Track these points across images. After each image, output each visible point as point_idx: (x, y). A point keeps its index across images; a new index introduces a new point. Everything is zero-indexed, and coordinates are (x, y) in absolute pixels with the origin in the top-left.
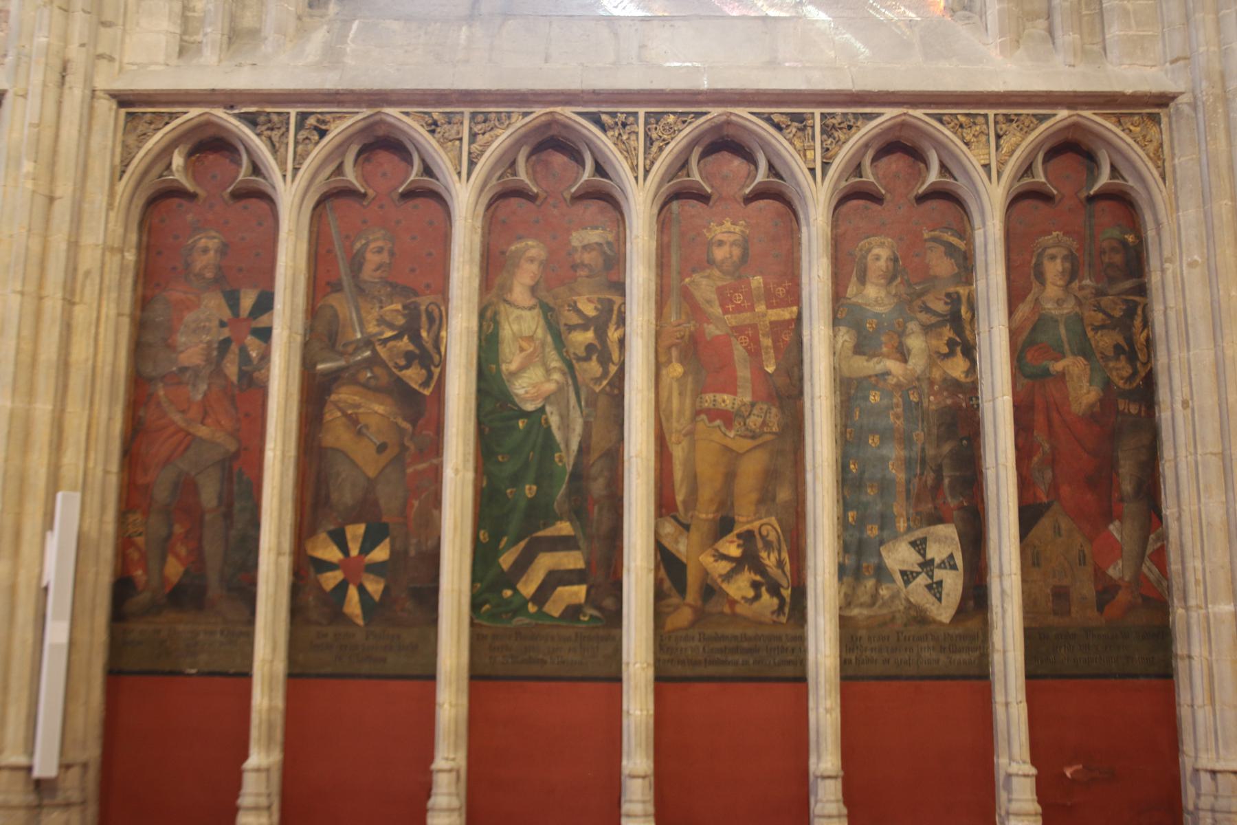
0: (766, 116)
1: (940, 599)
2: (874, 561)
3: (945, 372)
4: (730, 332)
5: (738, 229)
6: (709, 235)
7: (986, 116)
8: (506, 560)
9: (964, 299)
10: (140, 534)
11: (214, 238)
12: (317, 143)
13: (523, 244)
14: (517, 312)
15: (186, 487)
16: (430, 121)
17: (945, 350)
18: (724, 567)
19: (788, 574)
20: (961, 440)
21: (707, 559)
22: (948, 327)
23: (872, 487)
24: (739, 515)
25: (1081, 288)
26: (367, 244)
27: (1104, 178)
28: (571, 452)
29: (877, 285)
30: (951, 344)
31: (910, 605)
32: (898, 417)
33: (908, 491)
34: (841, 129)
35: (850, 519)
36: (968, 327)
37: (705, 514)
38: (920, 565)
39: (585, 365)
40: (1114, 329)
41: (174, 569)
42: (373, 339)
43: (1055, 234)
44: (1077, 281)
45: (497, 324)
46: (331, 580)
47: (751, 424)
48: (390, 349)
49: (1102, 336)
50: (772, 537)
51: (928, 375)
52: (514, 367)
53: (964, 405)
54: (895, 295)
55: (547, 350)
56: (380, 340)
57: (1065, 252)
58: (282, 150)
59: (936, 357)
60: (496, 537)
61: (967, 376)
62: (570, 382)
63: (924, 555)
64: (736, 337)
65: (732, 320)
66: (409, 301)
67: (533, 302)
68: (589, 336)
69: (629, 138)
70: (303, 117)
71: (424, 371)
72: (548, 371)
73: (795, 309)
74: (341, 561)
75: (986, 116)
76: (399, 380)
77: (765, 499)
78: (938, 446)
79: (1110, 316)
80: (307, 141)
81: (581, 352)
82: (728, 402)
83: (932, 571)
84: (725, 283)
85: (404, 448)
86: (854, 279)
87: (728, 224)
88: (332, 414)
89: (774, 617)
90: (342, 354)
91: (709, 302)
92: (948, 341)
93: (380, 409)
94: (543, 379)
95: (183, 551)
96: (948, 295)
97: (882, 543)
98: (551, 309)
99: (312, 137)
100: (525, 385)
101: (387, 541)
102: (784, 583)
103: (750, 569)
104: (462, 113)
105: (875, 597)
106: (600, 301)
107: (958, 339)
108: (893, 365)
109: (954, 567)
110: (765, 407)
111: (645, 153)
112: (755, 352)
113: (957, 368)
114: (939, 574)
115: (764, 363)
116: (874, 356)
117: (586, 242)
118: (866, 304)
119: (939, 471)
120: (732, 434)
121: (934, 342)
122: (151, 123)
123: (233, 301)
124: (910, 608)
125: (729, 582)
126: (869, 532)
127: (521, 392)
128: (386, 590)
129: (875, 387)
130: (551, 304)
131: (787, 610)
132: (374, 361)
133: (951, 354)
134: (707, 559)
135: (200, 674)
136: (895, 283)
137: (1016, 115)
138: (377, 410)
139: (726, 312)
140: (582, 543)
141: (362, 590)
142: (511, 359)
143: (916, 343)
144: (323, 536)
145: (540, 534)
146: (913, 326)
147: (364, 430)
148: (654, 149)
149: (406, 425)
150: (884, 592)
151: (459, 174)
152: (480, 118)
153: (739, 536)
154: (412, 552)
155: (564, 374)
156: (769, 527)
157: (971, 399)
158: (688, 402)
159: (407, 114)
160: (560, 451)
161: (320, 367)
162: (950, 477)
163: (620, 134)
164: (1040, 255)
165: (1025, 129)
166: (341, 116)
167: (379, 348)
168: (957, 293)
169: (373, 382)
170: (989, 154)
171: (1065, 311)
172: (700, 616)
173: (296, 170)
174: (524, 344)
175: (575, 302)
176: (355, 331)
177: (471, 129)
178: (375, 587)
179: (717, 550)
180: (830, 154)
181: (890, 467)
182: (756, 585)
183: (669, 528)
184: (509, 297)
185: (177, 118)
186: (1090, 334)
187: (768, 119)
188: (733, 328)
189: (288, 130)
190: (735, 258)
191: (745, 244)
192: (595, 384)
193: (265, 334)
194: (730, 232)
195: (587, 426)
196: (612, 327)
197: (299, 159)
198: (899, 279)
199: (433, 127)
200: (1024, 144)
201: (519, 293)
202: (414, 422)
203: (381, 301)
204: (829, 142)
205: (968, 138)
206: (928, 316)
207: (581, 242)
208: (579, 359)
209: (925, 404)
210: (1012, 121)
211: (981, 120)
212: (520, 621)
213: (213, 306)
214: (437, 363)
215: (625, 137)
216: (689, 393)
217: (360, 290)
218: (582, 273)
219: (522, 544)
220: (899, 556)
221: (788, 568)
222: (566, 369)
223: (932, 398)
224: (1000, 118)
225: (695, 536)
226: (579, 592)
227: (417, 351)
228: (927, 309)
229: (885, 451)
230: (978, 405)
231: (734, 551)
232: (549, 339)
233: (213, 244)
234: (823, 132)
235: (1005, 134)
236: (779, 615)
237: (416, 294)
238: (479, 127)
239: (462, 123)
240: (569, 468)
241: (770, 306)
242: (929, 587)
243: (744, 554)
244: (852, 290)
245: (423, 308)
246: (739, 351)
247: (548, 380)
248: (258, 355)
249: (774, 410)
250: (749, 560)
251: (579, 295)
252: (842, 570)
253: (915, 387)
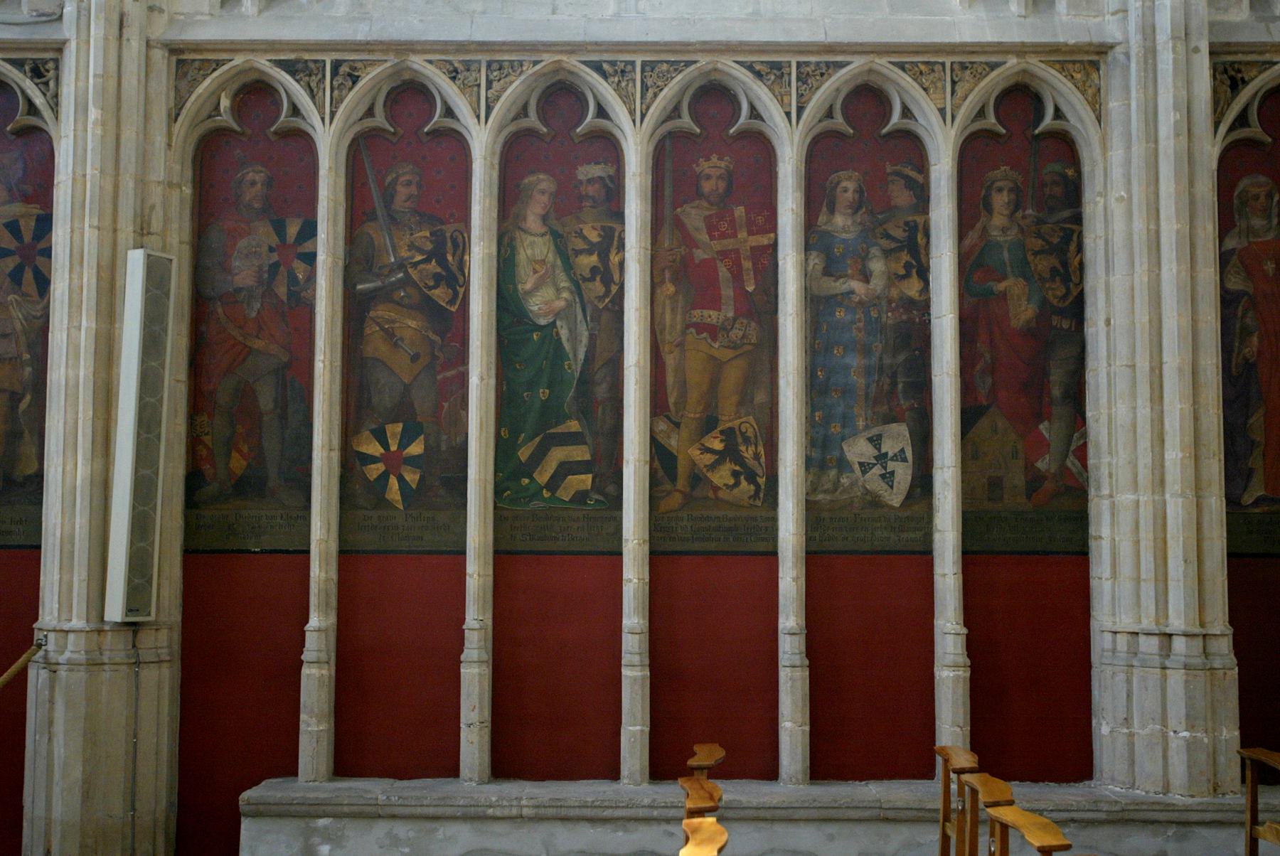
0: (749, 64)
1: (892, 487)
2: (836, 454)
3: (902, 292)
4: (716, 256)
5: (723, 164)
6: (698, 170)
7: (943, 64)
8: (524, 454)
9: (921, 227)
10: (207, 434)
11: (261, 172)
12: (350, 89)
13: (535, 178)
14: (530, 239)
15: (246, 394)
16: (451, 69)
17: (902, 272)
18: (709, 459)
19: (764, 465)
20: (914, 351)
21: (695, 453)
22: (906, 252)
23: (836, 391)
24: (722, 415)
25: (1024, 217)
26: (397, 178)
27: (1048, 121)
28: (579, 360)
29: (844, 215)
30: (908, 266)
31: (868, 492)
32: (859, 330)
33: (867, 395)
34: (814, 76)
35: (817, 419)
36: (923, 251)
37: (693, 413)
38: (876, 458)
39: (590, 285)
40: (1051, 254)
41: (238, 464)
42: (406, 263)
43: (1003, 168)
44: (1021, 211)
45: (513, 249)
46: (374, 470)
47: (734, 337)
48: (420, 272)
49: (1040, 260)
50: (750, 433)
51: (887, 294)
52: (528, 286)
53: (917, 320)
54: (860, 224)
55: (558, 272)
56: (411, 263)
57: (1011, 185)
58: (321, 94)
59: (894, 278)
60: (515, 433)
61: (920, 296)
62: (577, 300)
63: (879, 450)
64: (722, 261)
65: (717, 245)
66: (435, 229)
67: (543, 230)
68: (594, 259)
69: (627, 85)
70: (336, 65)
72: (558, 290)
73: (772, 235)
74: (382, 454)
75: (943, 64)
76: (429, 298)
77: (745, 400)
78: (894, 356)
79: (1047, 241)
80: (342, 86)
81: (587, 274)
82: (713, 317)
83: (886, 463)
84: (711, 213)
85: (434, 357)
86: (824, 209)
87: (714, 158)
88: (371, 329)
89: (751, 502)
90: (378, 276)
91: (697, 229)
92: (905, 264)
94: (554, 298)
95: (245, 449)
96: (906, 224)
97: (843, 439)
98: (560, 236)
99: (346, 83)
100: (538, 303)
101: (422, 437)
102: (759, 472)
103: (730, 461)
104: (479, 62)
105: (837, 484)
106: (603, 228)
107: (914, 262)
108: (856, 285)
109: (905, 460)
110: (745, 321)
111: (642, 98)
112: (737, 276)
113: (912, 288)
114: (891, 466)
115: (745, 284)
116: (841, 277)
117: (590, 176)
118: (834, 231)
119: (894, 376)
120: (716, 345)
121: (893, 265)
122: (200, 70)
123: (280, 229)
124: (866, 494)
125: (713, 471)
126: (833, 430)
127: (536, 308)
128: (422, 479)
129: (840, 305)
130: (560, 231)
131: (761, 495)
132: (407, 282)
133: (907, 276)
134: (695, 453)
135: (261, 552)
136: (860, 213)
137: (970, 63)
138: (411, 325)
139: (712, 238)
140: (589, 439)
141: (401, 479)
142: (526, 281)
143: (877, 266)
144: (366, 434)
145: (552, 431)
146: (875, 251)
147: (400, 343)
148: (650, 94)
150: (845, 481)
151: (478, 117)
152: (495, 66)
153: (722, 432)
154: (444, 448)
155: (572, 292)
156: (748, 425)
157: (924, 315)
158: (679, 318)
159: (430, 62)
160: (569, 359)
161: (359, 287)
162: (904, 382)
163: (619, 81)
164: (990, 188)
165: (978, 76)
166: (373, 63)
167: (410, 270)
168: (915, 221)
169: (406, 301)
170: (945, 98)
171: (1009, 238)
172: (688, 499)
173: (333, 114)
174: (537, 267)
175: (581, 230)
177: (487, 76)
178: (412, 477)
179: (703, 445)
180: (803, 100)
181: (852, 373)
182: (735, 474)
183: (662, 426)
184: (523, 225)
185: (223, 65)
186: (1030, 258)
187: (750, 67)
188: (718, 252)
189: (324, 76)
190: (721, 191)
191: (730, 177)
192: (599, 301)
193: (311, 258)
194: (716, 167)
195: (592, 338)
196: (613, 251)
197: (335, 104)
198: (864, 210)
199: (454, 74)
200: (977, 89)
201: (533, 221)
203: (411, 229)
204: (803, 88)
205: (927, 85)
206: (888, 242)
207: (586, 176)
208: (585, 280)
209: (884, 319)
210: (967, 68)
211: (937, 68)
212: (535, 504)
213: (264, 234)
214: (461, 283)
215: (623, 84)
216: (679, 310)
217: (392, 219)
218: (588, 204)
219: (538, 439)
220: (858, 450)
221: (763, 460)
222: (573, 288)
223: (890, 314)
224: (956, 67)
225: (685, 433)
226: (586, 480)
227: (444, 273)
228: (888, 236)
229: (848, 360)
230: (930, 321)
231: (718, 445)
232: (559, 262)
233: (259, 178)
234: (798, 79)
235: (960, 80)
236: (755, 500)
237: (442, 223)
238: (495, 74)
239: (479, 71)
240: (577, 375)
241: (750, 233)
242: (883, 476)
243: (725, 446)
244: (822, 218)
245: (448, 235)
246: (723, 272)
247: (558, 298)
248: (303, 278)
249: (753, 324)
250: (730, 453)
251: (585, 223)
252: (809, 463)
253: (875, 305)
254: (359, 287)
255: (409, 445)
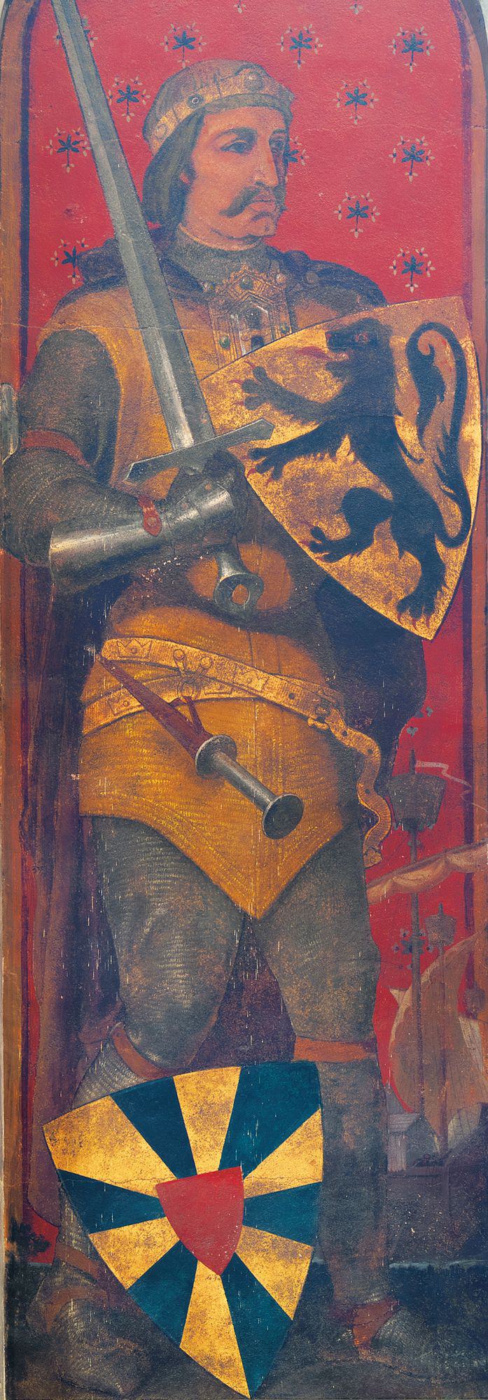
26: (197, 121)
48: (295, 488)
56: (257, 453)
66: (348, 320)
71: (411, 560)
74: (161, 1187)
76: (330, 589)
85: (357, 818)
90: (133, 502)
93: (271, 686)
128: (317, 1280)
147: (220, 758)
149: (362, 742)
154: (398, 1160)
161: (60, 546)
167: (256, 481)
169: (242, 599)
176: (173, 422)
202: (385, 734)
203: (255, 321)
214: (453, 532)
227: (386, 493)
237: (376, 298)
245: (399, 342)
254: (60, 546)
255: (267, 1147)
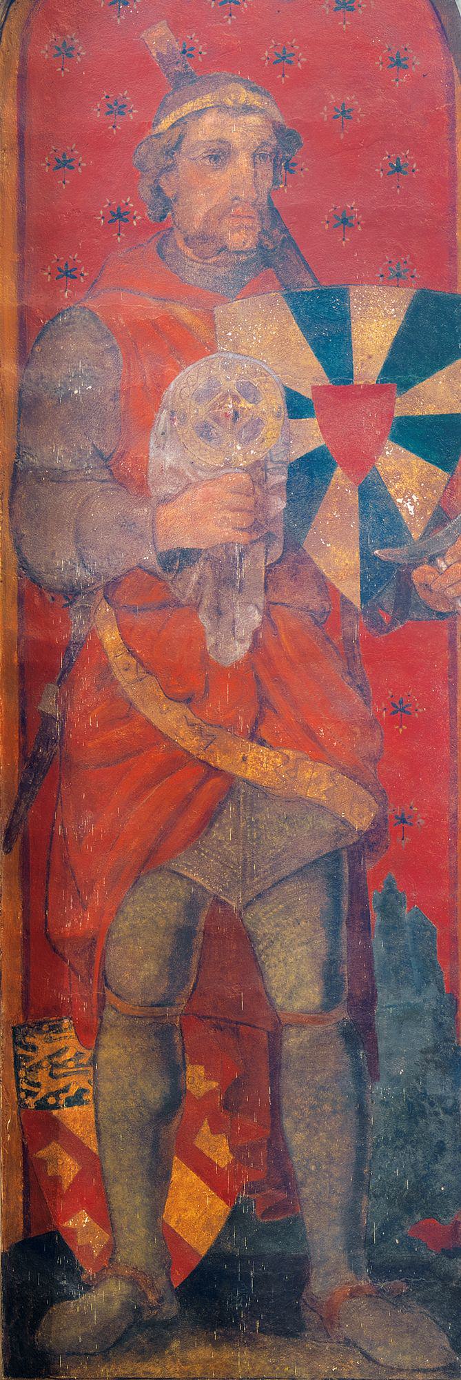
10: (77, 1100)
11: (248, 109)
248: (419, 513)
